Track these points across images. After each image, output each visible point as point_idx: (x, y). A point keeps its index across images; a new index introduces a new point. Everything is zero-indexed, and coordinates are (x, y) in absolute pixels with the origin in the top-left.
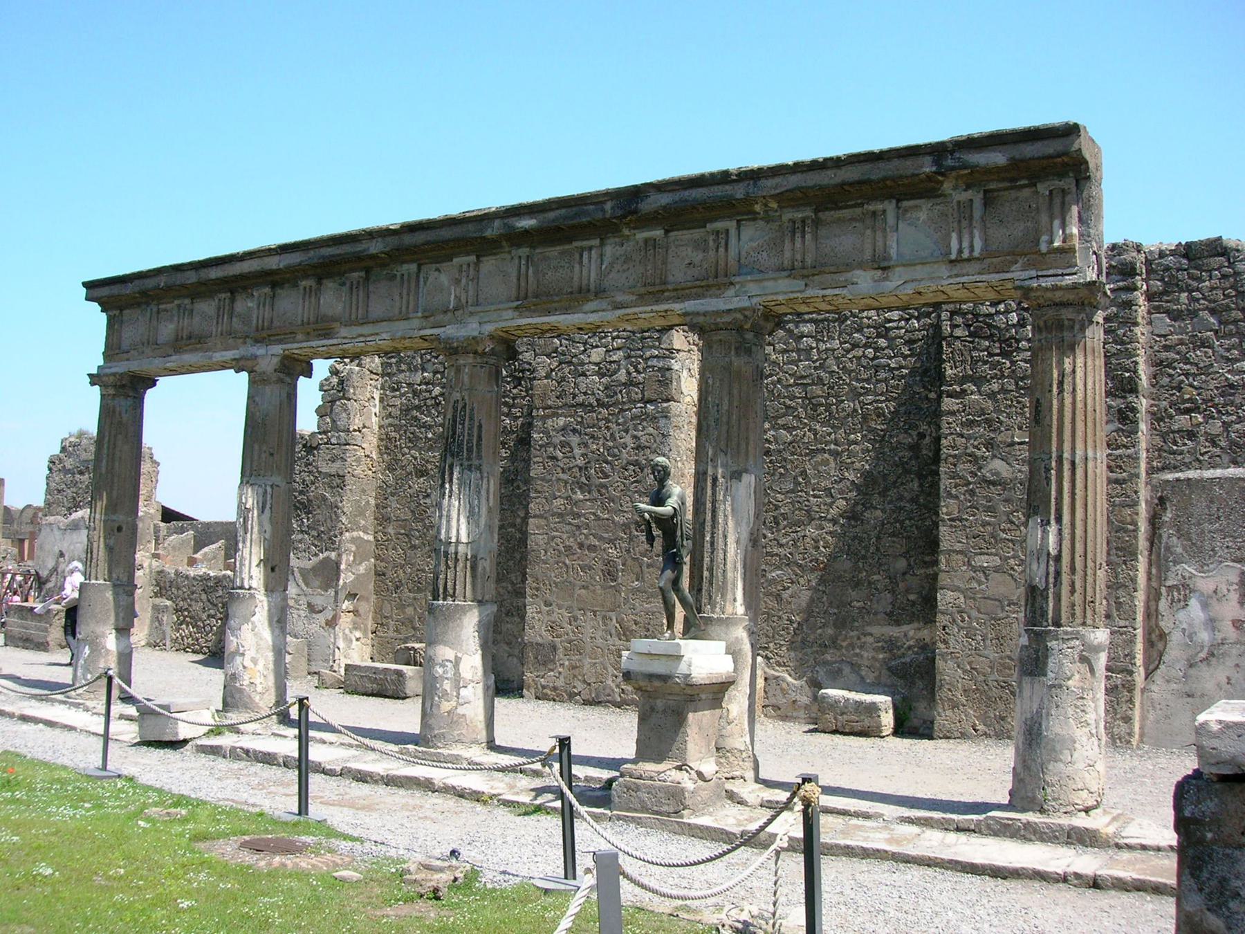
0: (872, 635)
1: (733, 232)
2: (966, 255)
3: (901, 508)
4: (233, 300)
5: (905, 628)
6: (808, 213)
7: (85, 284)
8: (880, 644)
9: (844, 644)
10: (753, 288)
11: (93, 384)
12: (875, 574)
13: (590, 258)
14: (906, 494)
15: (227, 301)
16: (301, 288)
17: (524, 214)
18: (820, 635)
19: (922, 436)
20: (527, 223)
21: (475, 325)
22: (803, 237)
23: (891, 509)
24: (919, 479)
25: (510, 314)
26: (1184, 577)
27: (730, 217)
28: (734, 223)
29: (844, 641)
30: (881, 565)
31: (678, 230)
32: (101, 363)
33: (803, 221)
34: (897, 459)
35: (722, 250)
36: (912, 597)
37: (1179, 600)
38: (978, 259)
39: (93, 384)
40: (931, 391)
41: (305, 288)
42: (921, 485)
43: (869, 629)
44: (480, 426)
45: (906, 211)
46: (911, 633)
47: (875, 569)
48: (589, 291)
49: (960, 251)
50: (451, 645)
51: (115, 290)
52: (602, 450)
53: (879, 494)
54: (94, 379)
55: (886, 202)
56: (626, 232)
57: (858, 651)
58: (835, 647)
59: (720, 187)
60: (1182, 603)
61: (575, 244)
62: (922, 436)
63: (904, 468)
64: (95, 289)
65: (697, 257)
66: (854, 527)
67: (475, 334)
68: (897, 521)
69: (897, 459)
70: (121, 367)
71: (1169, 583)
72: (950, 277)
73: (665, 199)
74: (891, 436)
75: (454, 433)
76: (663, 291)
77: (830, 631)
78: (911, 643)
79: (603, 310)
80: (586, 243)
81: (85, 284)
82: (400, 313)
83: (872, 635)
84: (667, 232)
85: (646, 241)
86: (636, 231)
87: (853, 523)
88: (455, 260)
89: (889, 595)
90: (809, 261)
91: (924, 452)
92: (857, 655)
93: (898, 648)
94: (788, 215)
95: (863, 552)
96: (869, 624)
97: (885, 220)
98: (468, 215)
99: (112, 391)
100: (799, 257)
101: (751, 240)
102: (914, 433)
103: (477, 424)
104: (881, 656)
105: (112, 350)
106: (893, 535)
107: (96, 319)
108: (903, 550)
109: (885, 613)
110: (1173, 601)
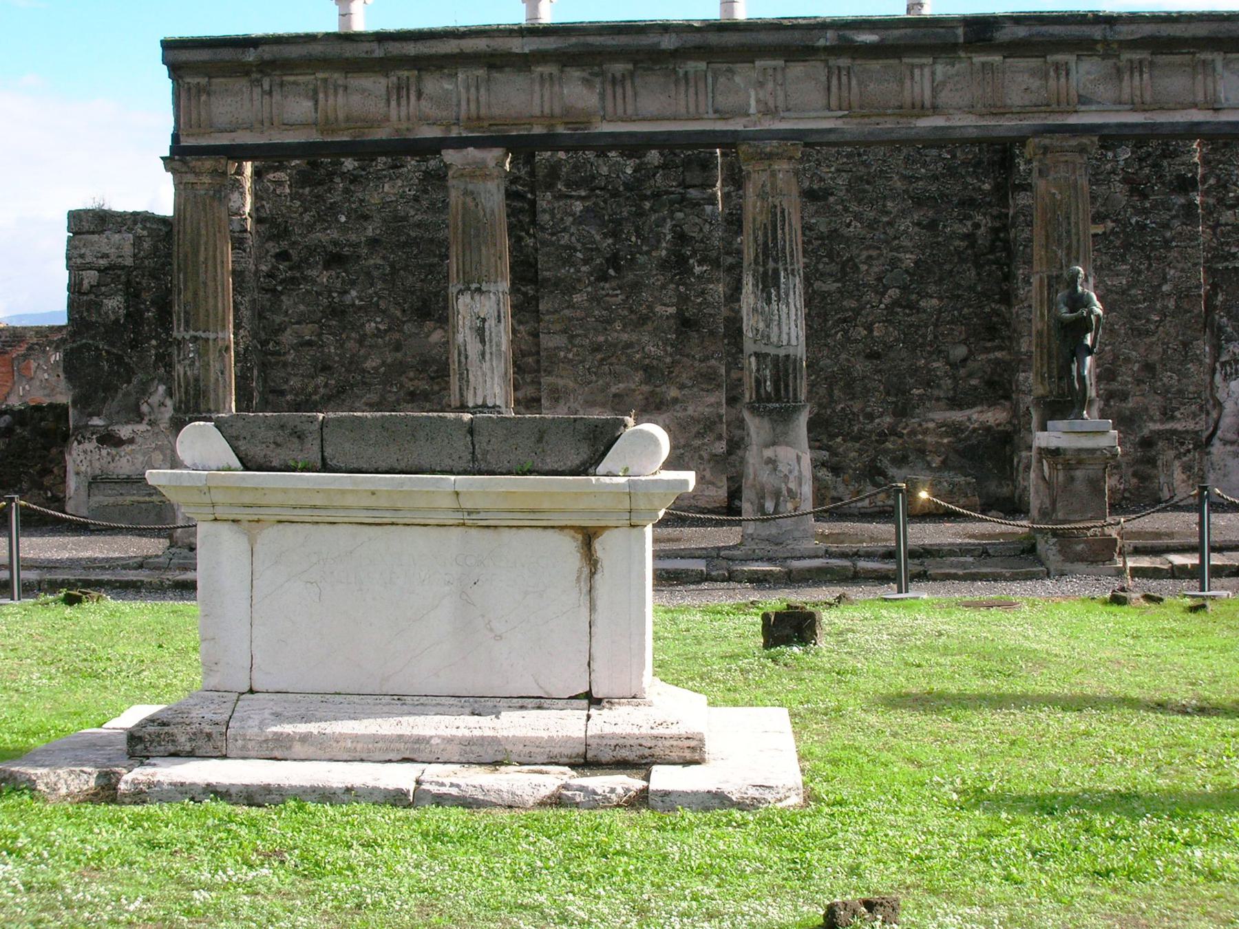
0: (933, 420)
1: (1073, 66)
3: (959, 296)
4: (419, 79)
5: (968, 412)
6: (1143, 55)
8: (943, 429)
9: (905, 432)
12: (934, 361)
13: (922, 75)
14: (962, 282)
15: (412, 80)
16: (536, 75)
17: (864, 29)
18: (879, 424)
19: (977, 226)
22: (1141, 75)
23: (947, 297)
24: (976, 268)
26: (1234, 354)
27: (1071, 52)
28: (1075, 58)
29: (904, 428)
30: (940, 352)
31: (1014, 57)
33: (1141, 62)
34: (952, 248)
35: (1063, 80)
36: (974, 382)
37: (1231, 374)
40: (984, 183)
41: (542, 75)
42: (978, 274)
43: (931, 415)
45: (1230, 62)
46: (975, 417)
47: (934, 357)
48: (923, 107)
51: (226, 54)
52: (633, 239)
53: (935, 282)
55: (1215, 53)
56: (963, 55)
57: (920, 437)
58: (896, 434)
59: (1077, 27)
60: (1234, 376)
61: (905, 60)
62: (977, 226)
63: (960, 257)
65: (1035, 83)
66: (908, 315)
68: (954, 308)
69: (952, 248)
71: (1223, 359)
73: (1021, 32)
74: (945, 226)
75: (775, 238)
77: (888, 419)
78: (976, 426)
80: (916, 61)
82: (688, 112)
83: (933, 420)
84: (1005, 57)
85: (983, 64)
86: (973, 55)
87: (907, 311)
88: (757, 63)
89: (949, 382)
90: (1148, 98)
91: (980, 242)
92: (920, 441)
93: (962, 431)
94: (1126, 56)
95: (920, 340)
96: (930, 410)
97: (1214, 70)
98: (800, 21)
100: (1138, 93)
101: (1088, 73)
102: (969, 223)
104: (945, 441)
106: (952, 322)
108: (963, 337)
109: (948, 399)
110: (1226, 374)
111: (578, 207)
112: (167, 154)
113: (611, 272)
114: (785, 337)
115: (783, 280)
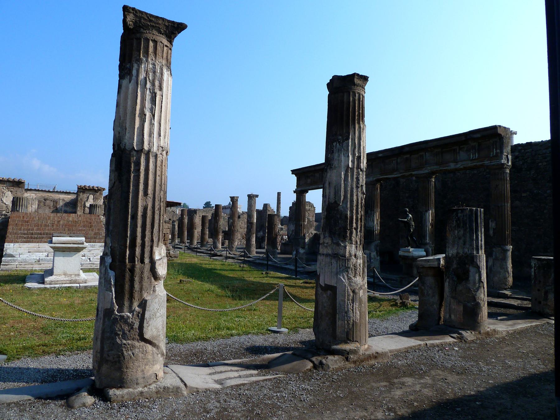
1: (424, 155)
2: (474, 158)
7: (291, 171)
10: (429, 168)
11: (294, 193)
20: (380, 155)
21: (372, 178)
25: (379, 176)
32: (296, 188)
38: (477, 159)
39: (294, 193)
44: (374, 201)
49: (473, 157)
50: (369, 250)
54: (295, 192)
64: (294, 172)
67: (372, 180)
70: (299, 189)
72: (471, 164)
76: (410, 169)
79: (398, 174)
80: (394, 159)
81: (291, 171)
99: (298, 195)
103: (373, 200)
105: (298, 185)
107: (294, 178)
111: (407, 195)
112: (295, 190)
113: (412, 209)
114: (369, 225)
115: (369, 212)
